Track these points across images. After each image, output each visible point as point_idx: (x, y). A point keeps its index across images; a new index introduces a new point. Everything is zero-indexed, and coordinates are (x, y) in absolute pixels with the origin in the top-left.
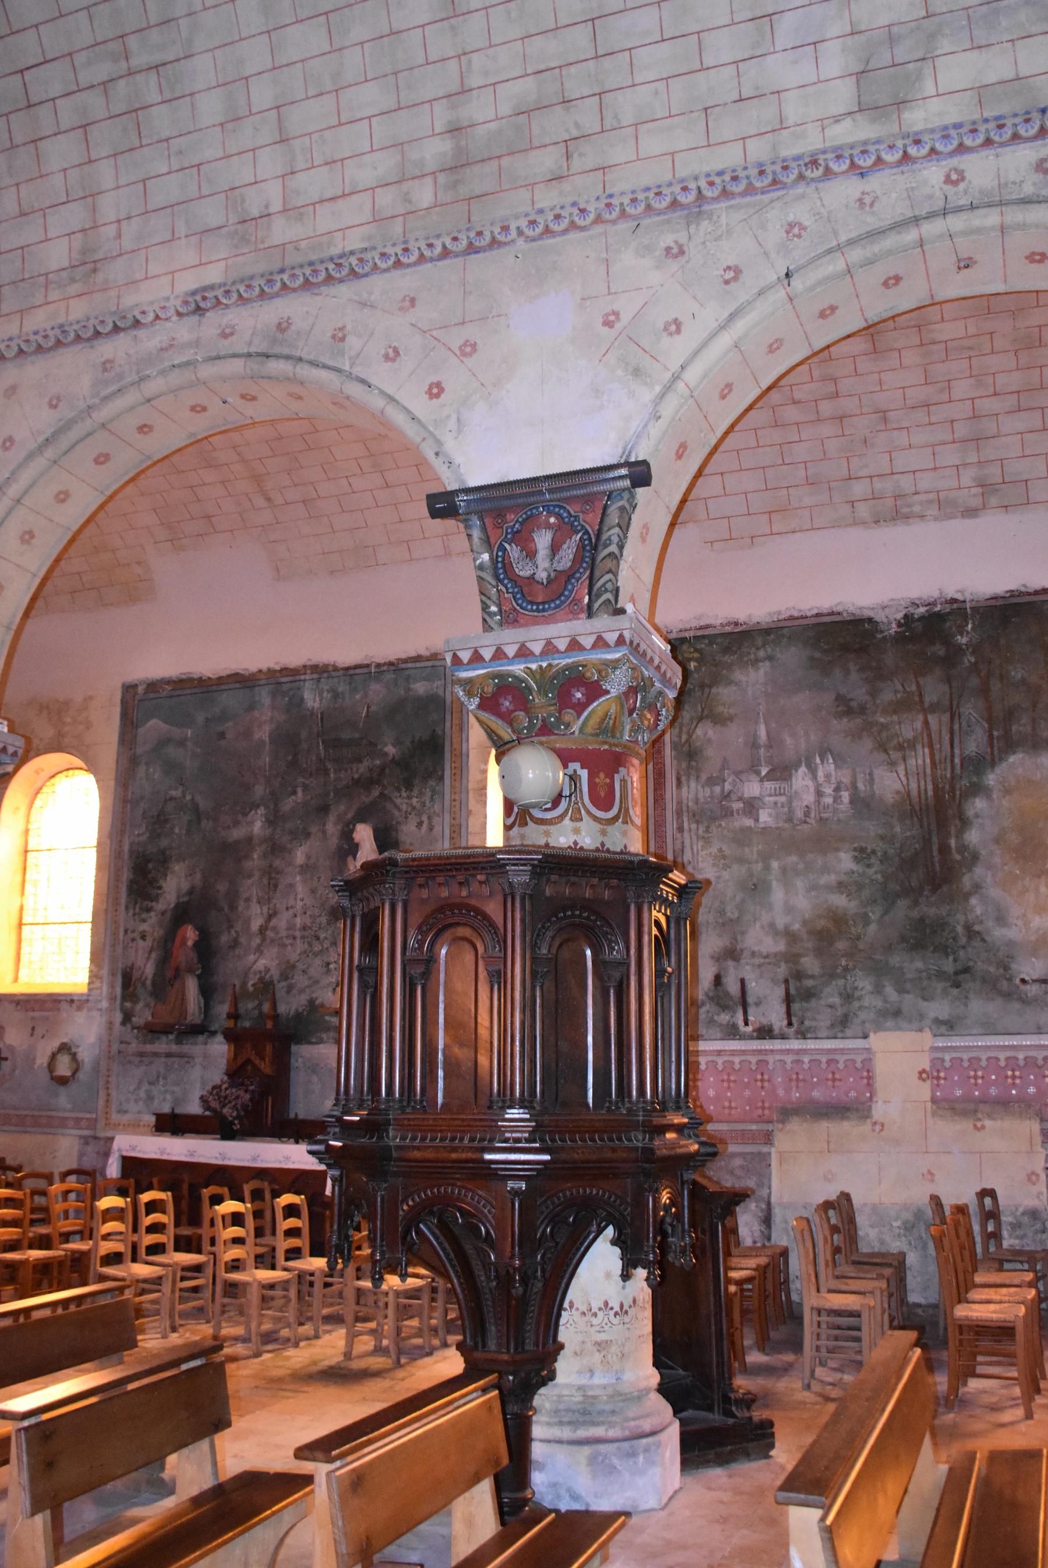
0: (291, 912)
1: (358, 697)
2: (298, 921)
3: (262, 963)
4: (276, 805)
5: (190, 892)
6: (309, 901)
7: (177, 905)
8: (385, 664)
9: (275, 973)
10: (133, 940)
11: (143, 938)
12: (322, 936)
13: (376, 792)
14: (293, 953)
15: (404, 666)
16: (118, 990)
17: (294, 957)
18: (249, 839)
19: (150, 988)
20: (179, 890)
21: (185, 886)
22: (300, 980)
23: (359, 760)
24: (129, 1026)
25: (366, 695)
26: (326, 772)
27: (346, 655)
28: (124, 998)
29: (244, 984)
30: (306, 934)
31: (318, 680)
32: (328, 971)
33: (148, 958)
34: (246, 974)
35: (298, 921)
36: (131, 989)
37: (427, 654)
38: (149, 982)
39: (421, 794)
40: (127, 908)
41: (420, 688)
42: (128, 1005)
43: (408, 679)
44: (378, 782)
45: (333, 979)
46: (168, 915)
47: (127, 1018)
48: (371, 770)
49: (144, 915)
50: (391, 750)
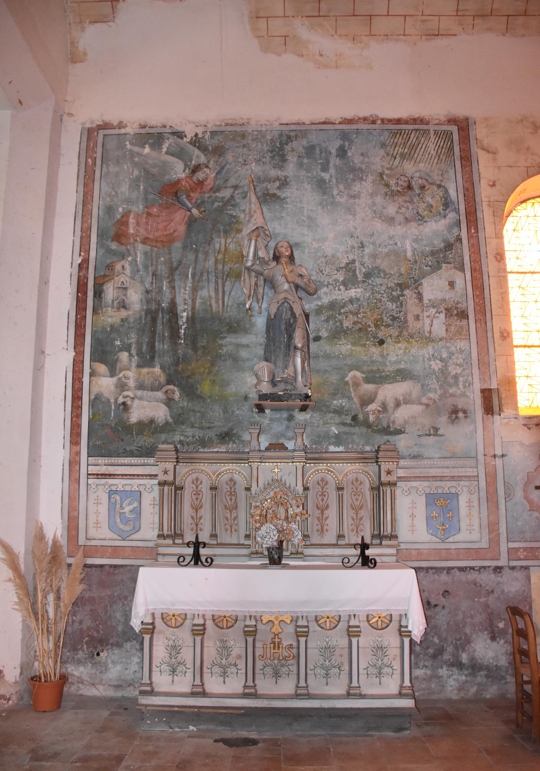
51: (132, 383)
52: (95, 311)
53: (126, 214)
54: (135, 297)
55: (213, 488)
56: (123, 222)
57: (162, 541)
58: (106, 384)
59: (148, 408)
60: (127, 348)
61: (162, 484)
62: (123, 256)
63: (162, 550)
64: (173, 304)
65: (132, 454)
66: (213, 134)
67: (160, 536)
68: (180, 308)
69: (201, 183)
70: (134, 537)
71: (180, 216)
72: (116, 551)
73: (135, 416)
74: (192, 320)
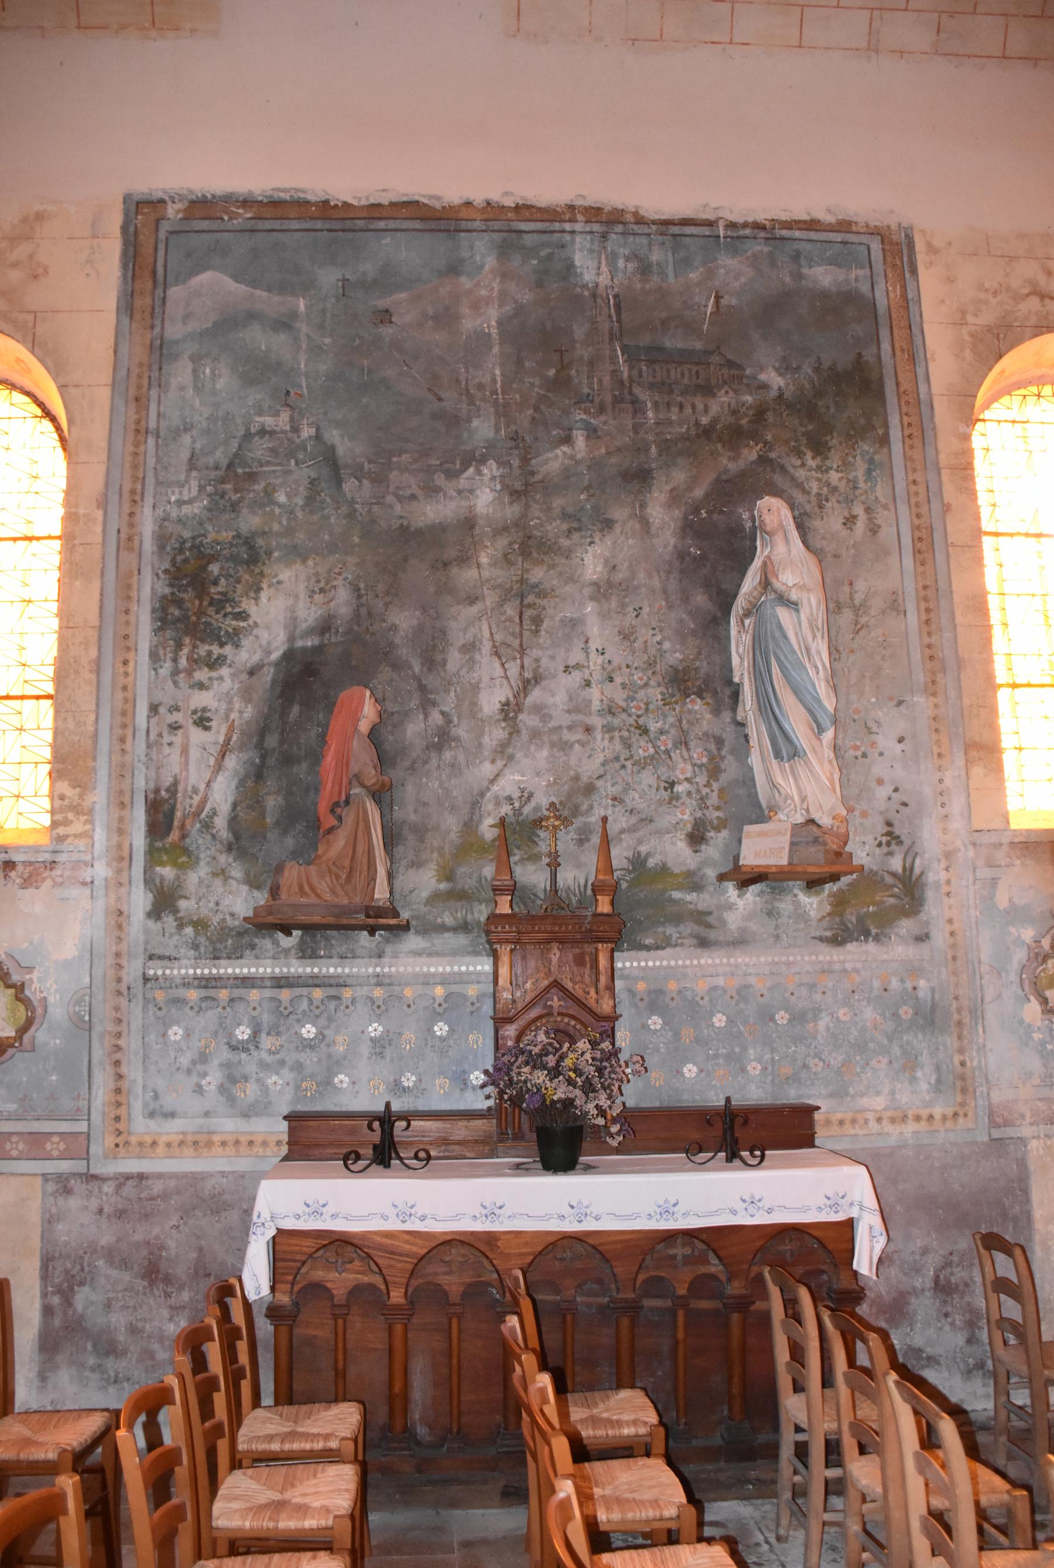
0: (577, 677)
1: (693, 276)
2: (595, 695)
3: (510, 783)
4: (525, 461)
5: (325, 627)
6: (618, 655)
7: (289, 655)
8: (745, 225)
10: (174, 727)
11: (202, 721)
12: (654, 727)
13: (750, 454)
14: (587, 764)
15: (785, 233)
16: (139, 839)
17: (590, 769)
18: (469, 523)
19: (224, 834)
20: (292, 622)
21: (309, 614)
23: (708, 390)
24: (169, 921)
25: (710, 274)
26: (637, 407)
27: (661, 197)
28: (153, 856)
29: (470, 826)
30: (616, 722)
31: (604, 236)
32: (674, 798)
33: (219, 767)
34: (475, 804)
35: (595, 695)
36: (174, 836)
37: (830, 219)
38: (221, 823)
39: (845, 466)
40: (155, 657)
41: (824, 276)
42: (167, 872)
43: (796, 257)
44: (755, 435)
45: (686, 815)
46: (268, 675)
47: (164, 902)
48: (734, 412)
49: (202, 675)
50: (775, 380)
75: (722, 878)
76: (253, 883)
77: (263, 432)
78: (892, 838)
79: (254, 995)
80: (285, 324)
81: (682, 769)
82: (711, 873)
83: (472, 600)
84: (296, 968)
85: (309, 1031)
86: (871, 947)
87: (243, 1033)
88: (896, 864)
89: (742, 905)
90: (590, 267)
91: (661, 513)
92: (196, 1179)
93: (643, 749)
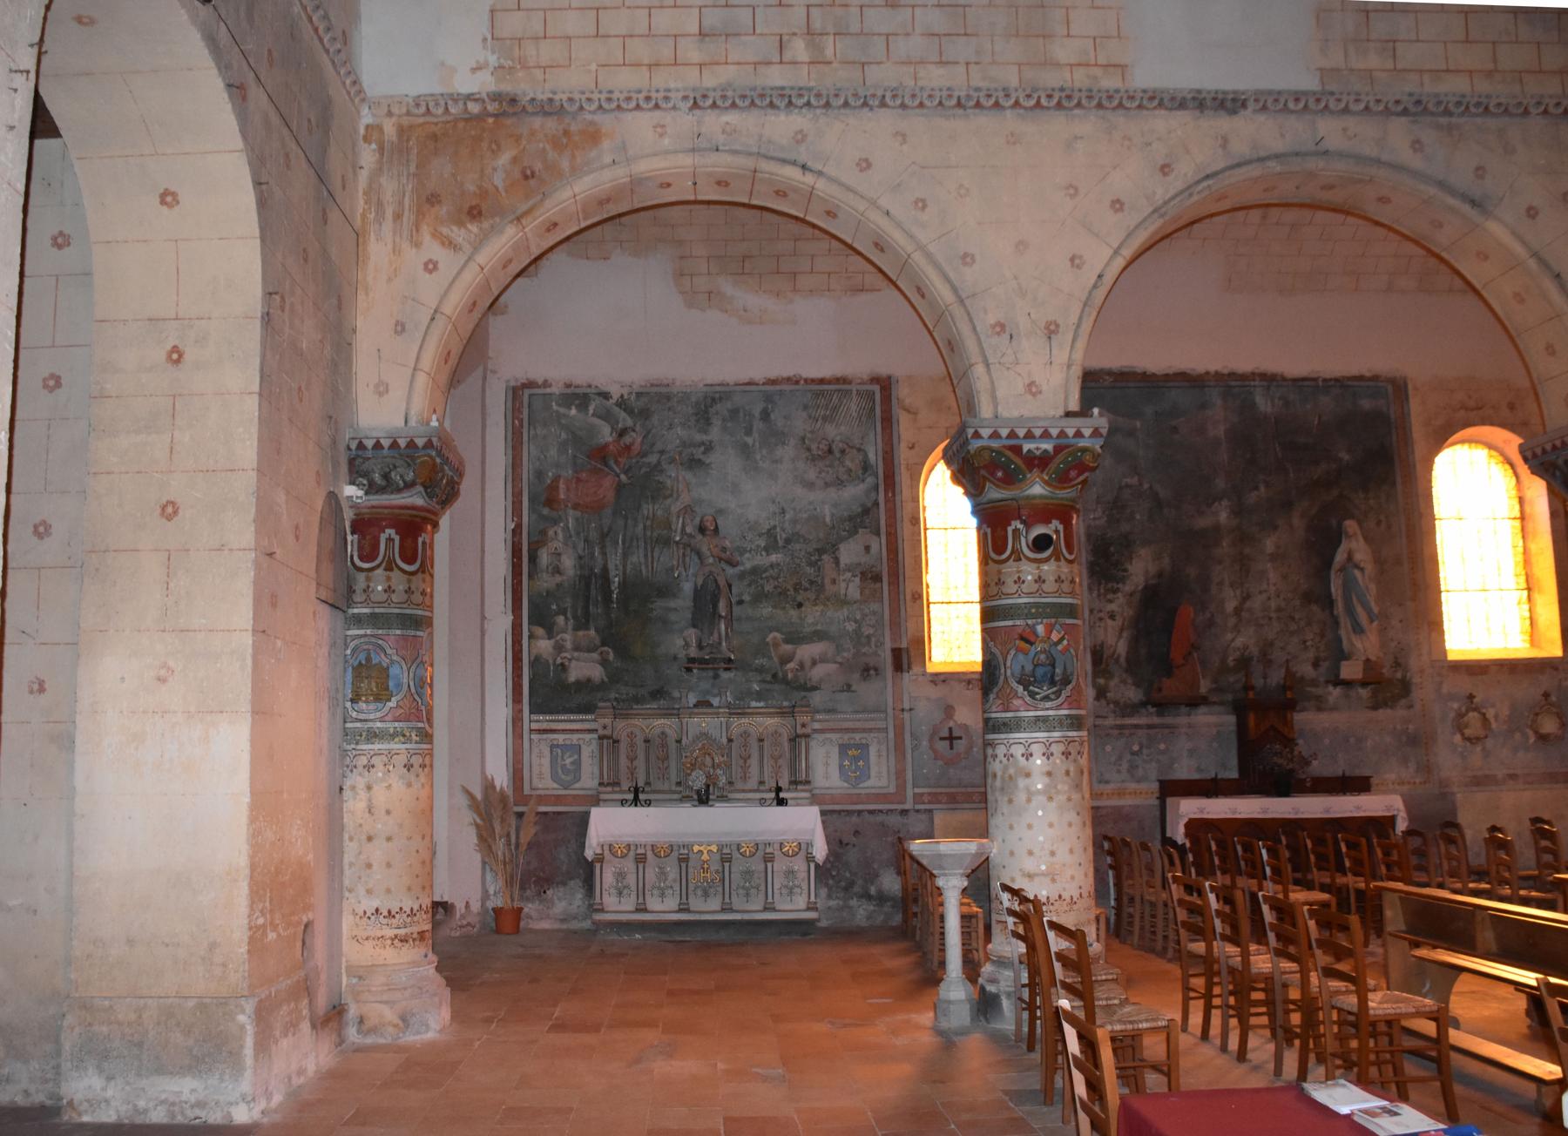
0: (1264, 596)
2: (1273, 604)
3: (1239, 642)
5: (1160, 575)
7: (1146, 588)
9: (1255, 651)
11: (1112, 616)
18: (1217, 528)
20: (1147, 572)
21: (1153, 569)
22: (1278, 656)
24: (1103, 702)
27: (1294, 365)
28: (1096, 674)
32: (1306, 648)
33: (1120, 637)
38: (1122, 660)
41: (1366, 404)
42: (1101, 681)
45: (1311, 654)
49: (1110, 596)
50: (1345, 456)
51: (569, 645)
52: (530, 577)
53: (557, 479)
54: (568, 563)
55: (647, 741)
56: (553, 488)
57: (603, 789)
58: (545, 646)
59: (584, 668)
60: (564, 612)
61: (601, 738)
62: (555, 522)
63: (603, 796)
64: (605, 569)
65: (571, 711)
66: (639, 395)
67: (601, 784)
68: (612, 573)
69: (628, 448)
70: (577, 785)
71: (608, 483)
72: (558, 799)
73: (573, 675)
74: (623, 585)
75: (1327, 682)
76: (1137, 685)
77: (1127, 486)
78: (1397, 664)
79: (1140, 732)
80: (1131, 433)
81: (1309, 636)
82: (1322, 679)
83: (1220, 562)
84: (1156, 720)
85: (1162, 746)
86: (1389, 711)
87: (1136, 748)
88: (1399, 675)
89: (1335, 693)
90: (1263, 404)
91: (1296, 521)
92: (1118, 809)
93: (1293, 627)
